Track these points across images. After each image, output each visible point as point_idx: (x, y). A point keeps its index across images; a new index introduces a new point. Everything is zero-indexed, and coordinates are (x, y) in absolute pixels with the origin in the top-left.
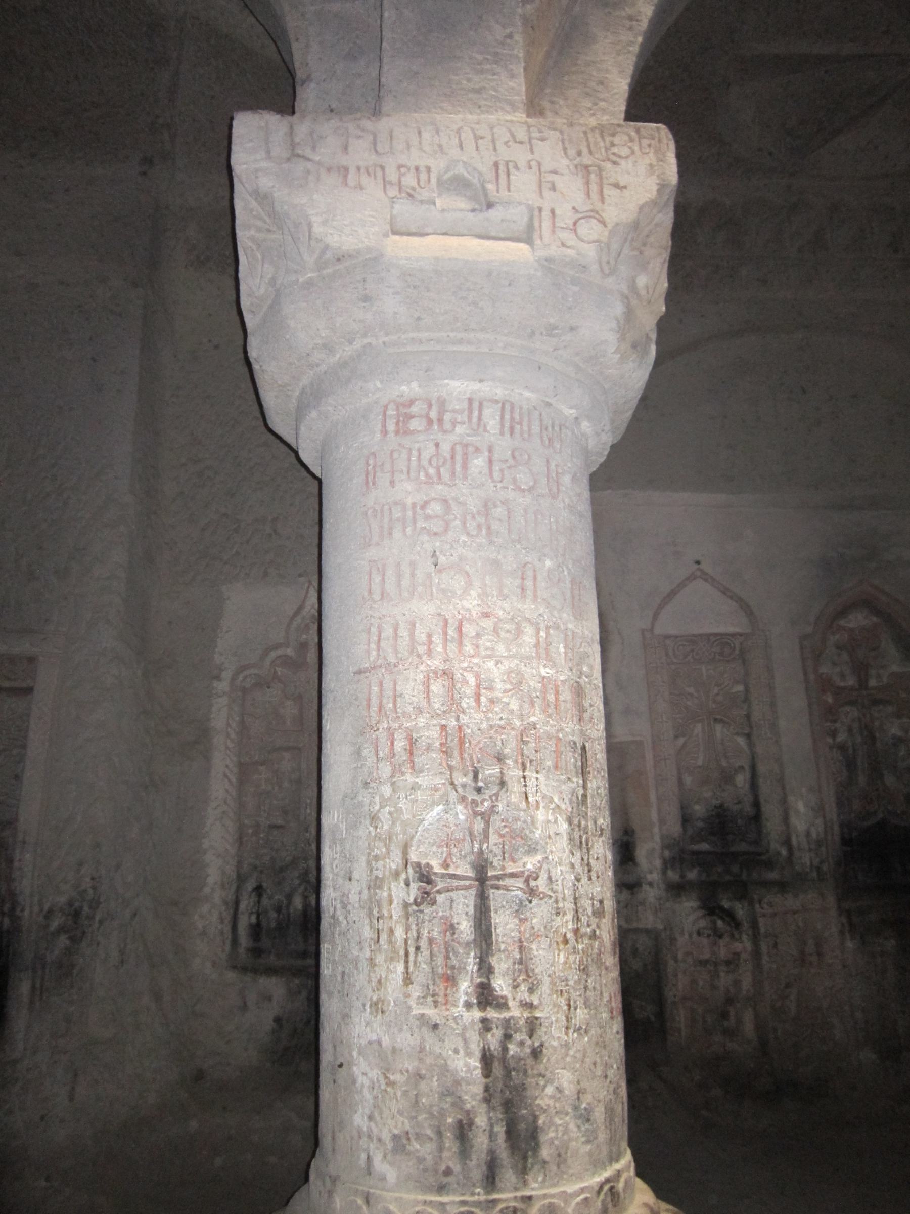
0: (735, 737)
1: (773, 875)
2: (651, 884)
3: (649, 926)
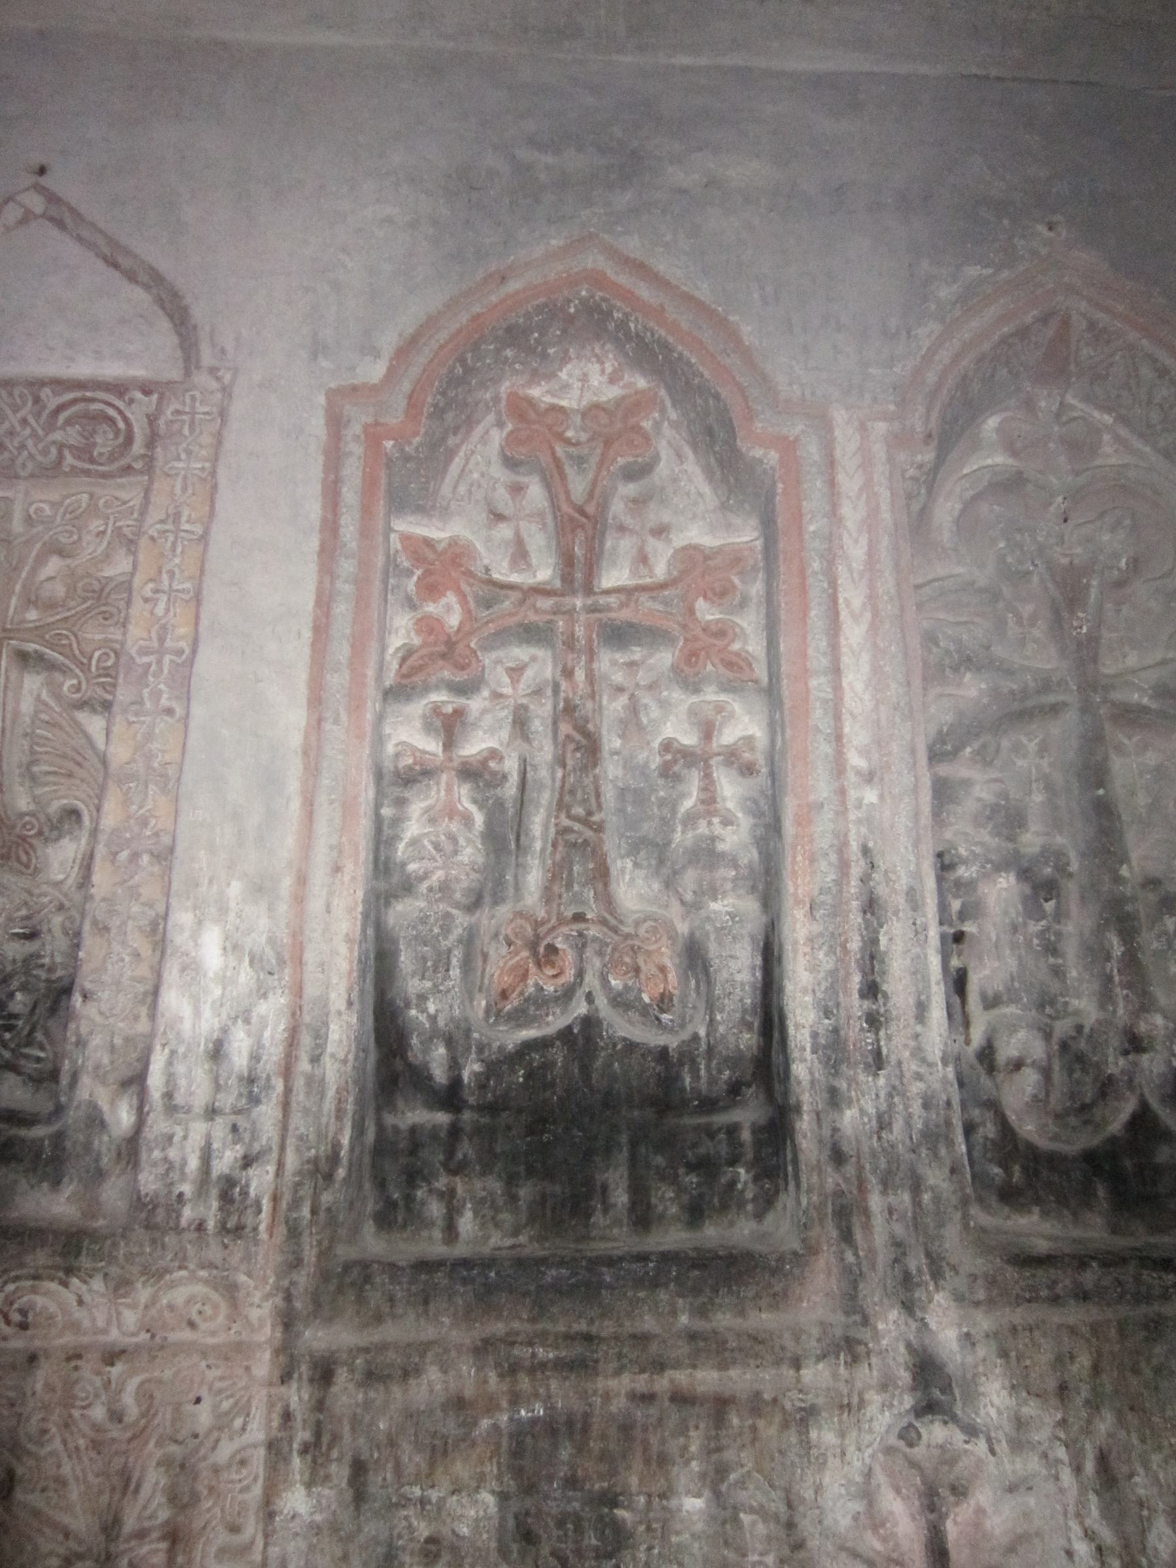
0: (82, 716)
1: (57, 1205)
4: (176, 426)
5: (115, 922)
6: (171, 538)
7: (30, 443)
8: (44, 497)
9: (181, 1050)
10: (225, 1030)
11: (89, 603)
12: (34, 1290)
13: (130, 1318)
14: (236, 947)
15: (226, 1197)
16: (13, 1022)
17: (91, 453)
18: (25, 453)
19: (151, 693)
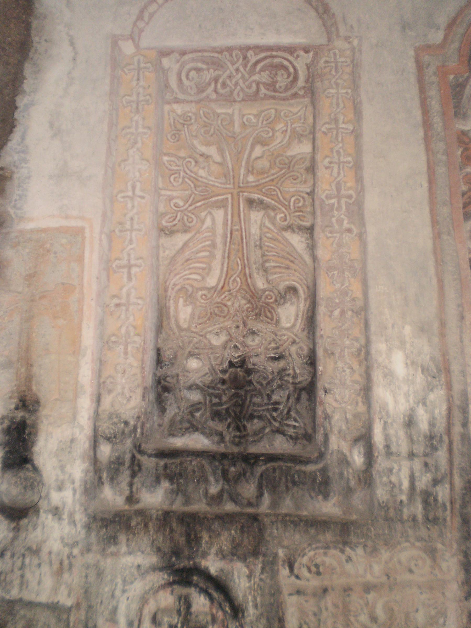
0: (288, 235)
1: (329, 507)
2: (56, 512)
3: (43, 598)
4: (327, 70)
5: (337, 351)
6: (335, 133)
7: (241, 82)
8: (248, 112)
9: (389, 421)
10: (412, 410)
11: (283, 171)
12: (325, 554)
13: (377, 568)
14: (413, 363)
15: (426, 503)
16: (277, 406)
17: (275, 86)
18: (238, 87)
19: (337, 221)
